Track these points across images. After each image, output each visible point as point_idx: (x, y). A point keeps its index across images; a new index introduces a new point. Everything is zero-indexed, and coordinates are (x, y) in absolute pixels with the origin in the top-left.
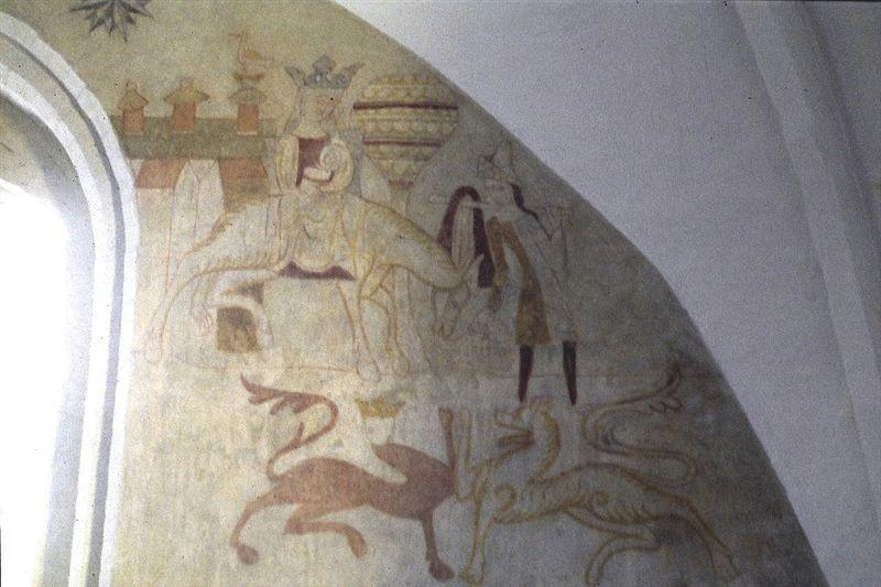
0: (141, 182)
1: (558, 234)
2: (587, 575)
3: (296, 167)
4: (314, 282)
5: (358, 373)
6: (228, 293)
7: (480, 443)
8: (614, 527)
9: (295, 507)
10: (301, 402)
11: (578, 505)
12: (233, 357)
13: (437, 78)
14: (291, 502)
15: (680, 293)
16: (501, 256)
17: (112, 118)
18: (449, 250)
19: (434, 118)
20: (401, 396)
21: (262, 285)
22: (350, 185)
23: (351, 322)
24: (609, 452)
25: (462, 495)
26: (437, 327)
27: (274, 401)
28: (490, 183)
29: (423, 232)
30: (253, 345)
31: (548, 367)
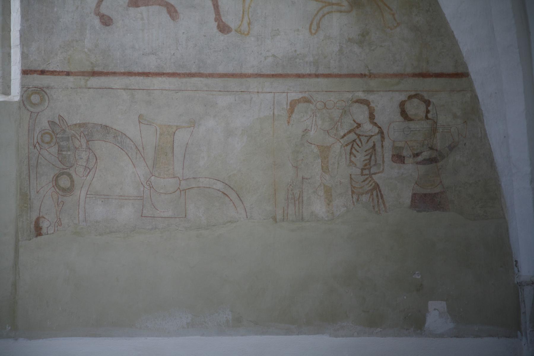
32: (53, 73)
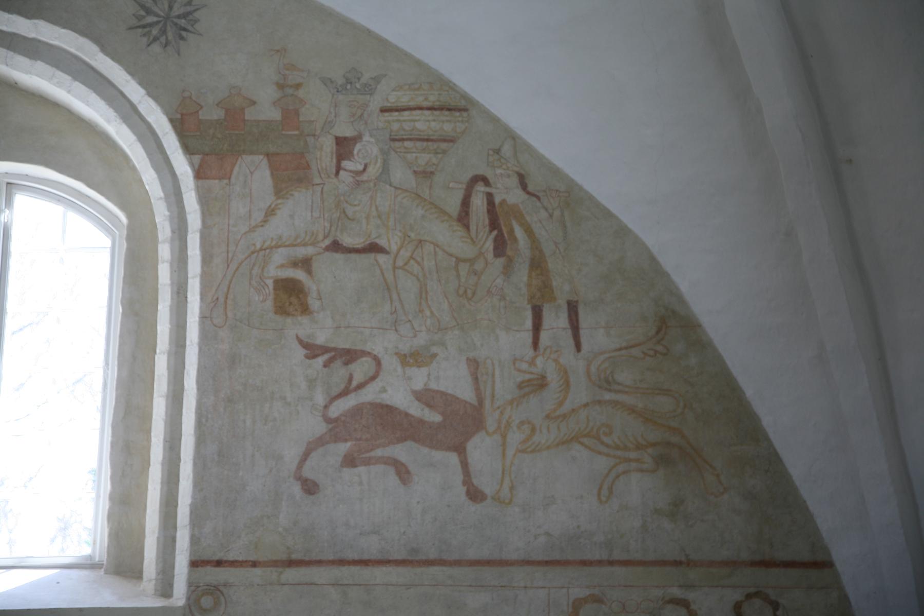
0: (199, 174)
1: (557, 213)
2: (599, 495)
3: (334, 161)
4: (353, 256)
5: (396, 330)
6: (282, 266)
7: (503, 387)
8: (619, 453)
9: (349, 444)
10: (350, 356)
11: (585, 436)
12: (289, 320)
13: (445, 84)
14: (346, 441)
15: (661, 259)
16: (511, 231)
17: (171, 121)
18: (467, 227)
19: (448, 118)
20: (434, 349)
21: (311, 259)
22: (381, 173)
23: (389, 289)
24: (610, 391)
25: (491, 429)
26: (461, 292)
27: (326, 356)
28: (499, 171)
29: (444, 213)
30: (305, 310)
31: (556, 322)
32: (233, 564)
